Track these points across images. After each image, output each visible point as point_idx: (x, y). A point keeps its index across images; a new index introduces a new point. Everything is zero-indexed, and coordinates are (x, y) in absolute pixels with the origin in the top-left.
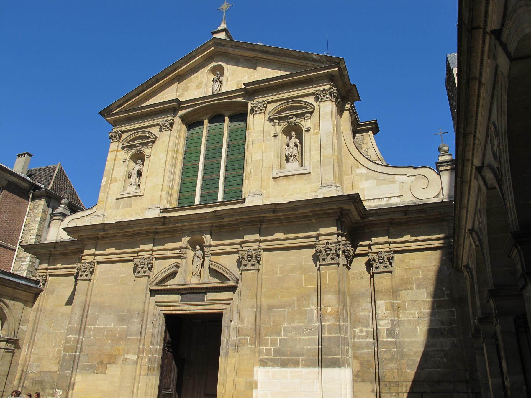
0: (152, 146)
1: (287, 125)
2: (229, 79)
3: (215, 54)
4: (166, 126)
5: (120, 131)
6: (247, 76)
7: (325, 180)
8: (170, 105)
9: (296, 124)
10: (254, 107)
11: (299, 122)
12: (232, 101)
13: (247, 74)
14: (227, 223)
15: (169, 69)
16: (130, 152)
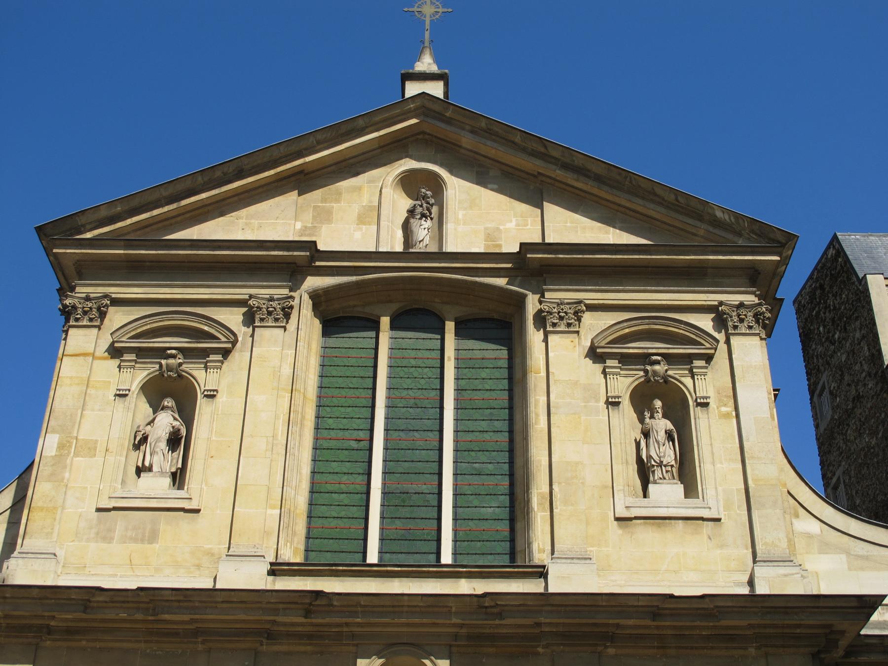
0: (222, 363)
1: (642, 379)
3: (412, 136)
4: (270, 313)
5: (106, 296)
6: (514, 220)
7: (766, 544)
8: (286, 253)
9: (666, 381)
10: (547, 312)
11: (677, 376)
12: (476, 282)
14: (505, 631)
15: (282, 148)
16: (145, 369)
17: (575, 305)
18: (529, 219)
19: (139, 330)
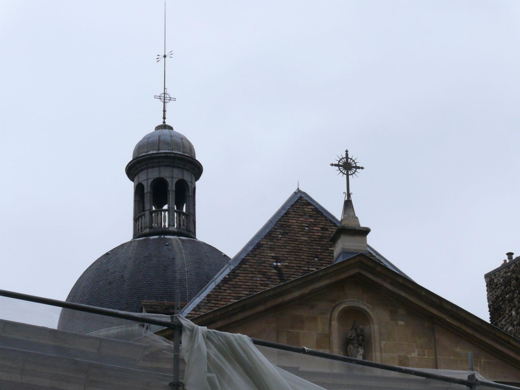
2: (382, 346)
18: (426, 350)
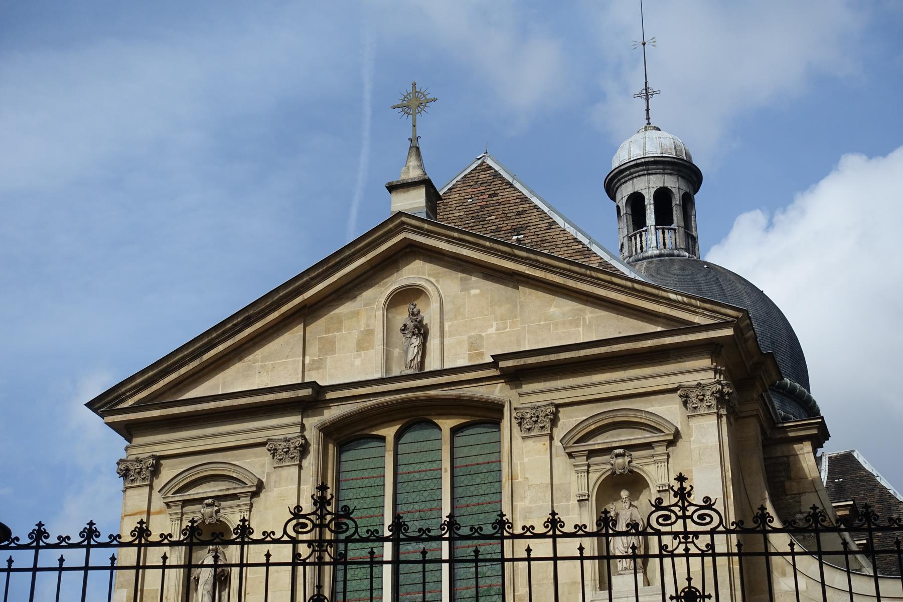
1: (609, 473)
6: (494, 324)
9: (631, 471)
10: (521, 418)
11: (639, 465)
13: (496, 320)
17: (546, 408)
18: (508, 321)
19: (181, 485)
